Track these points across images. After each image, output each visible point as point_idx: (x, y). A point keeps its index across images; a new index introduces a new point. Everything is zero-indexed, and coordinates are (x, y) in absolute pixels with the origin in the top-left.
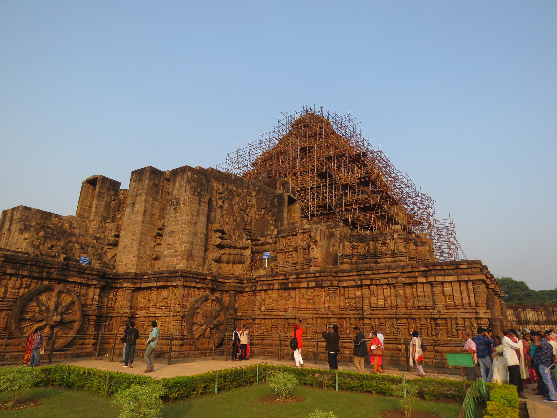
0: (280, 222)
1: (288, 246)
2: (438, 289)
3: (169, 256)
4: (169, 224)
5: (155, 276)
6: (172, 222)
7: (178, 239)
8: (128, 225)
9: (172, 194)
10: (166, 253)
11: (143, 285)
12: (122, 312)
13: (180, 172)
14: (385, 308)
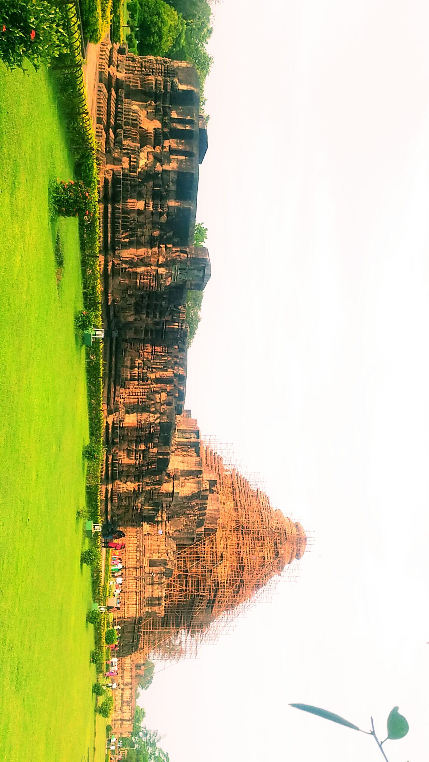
13: (199, 486)
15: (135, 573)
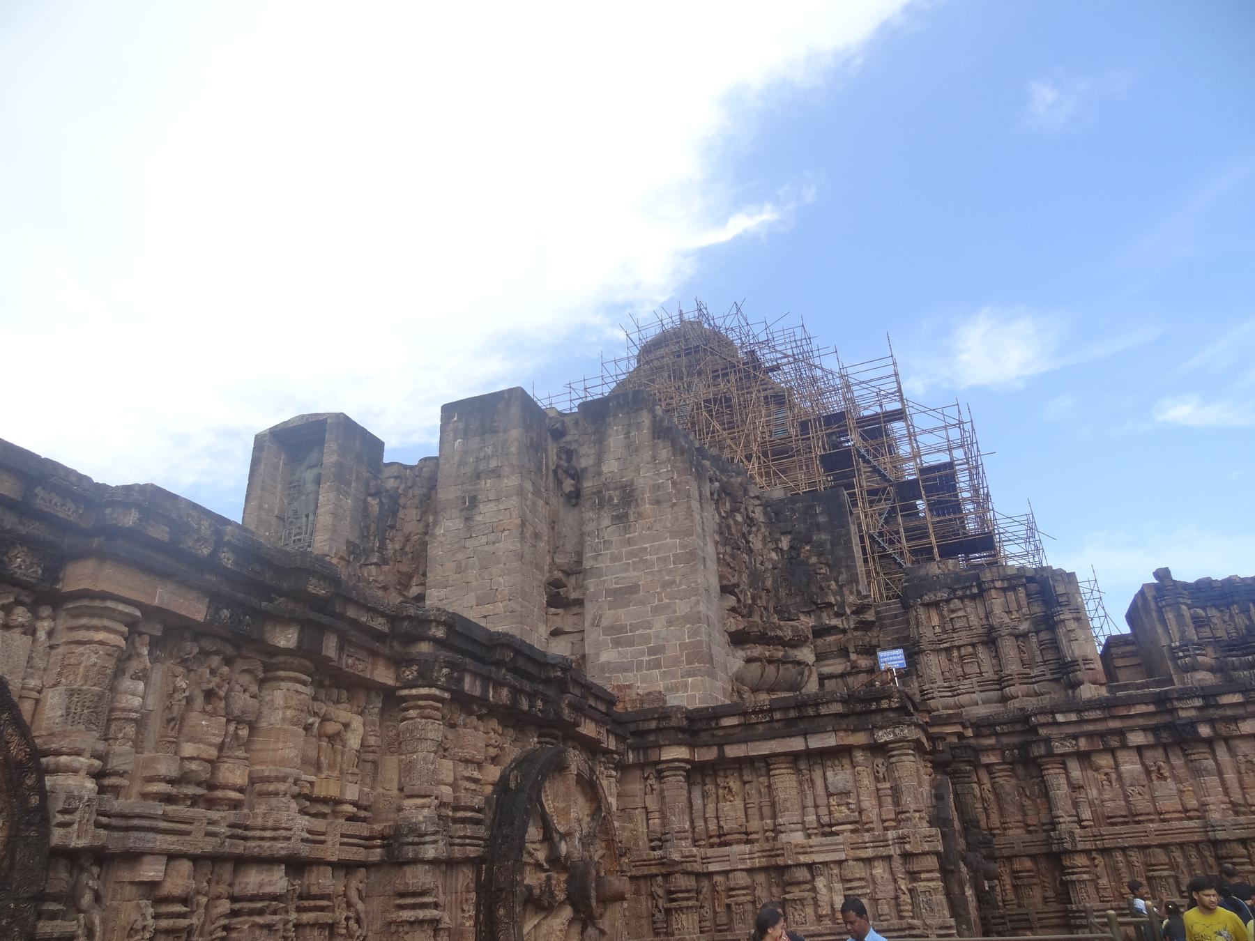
0: (843, 570)
1: (954, 630)
3: (626, 668)
4: (603, 564)
5: (778, 716)
6: (614, 558)
7: (657, 611)
8: (459, 570)
9: (599, 474)
10: (608, 655)
11: (732, 751)
12: (676, 856)
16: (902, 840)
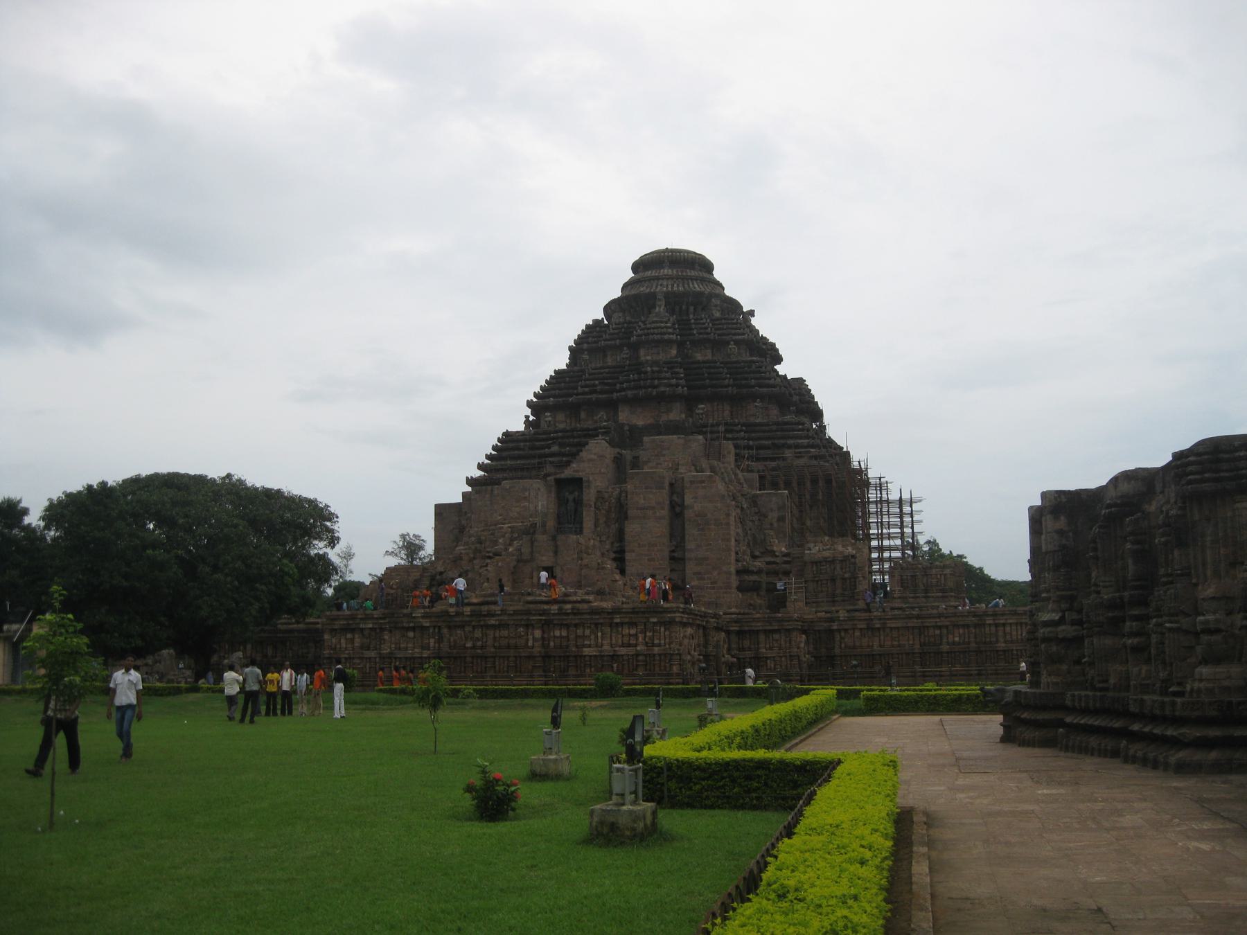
1: (821, 573)
2: (1001, 628)
14: (959, 643)
15: (931, 631)
16: (790, 652)
